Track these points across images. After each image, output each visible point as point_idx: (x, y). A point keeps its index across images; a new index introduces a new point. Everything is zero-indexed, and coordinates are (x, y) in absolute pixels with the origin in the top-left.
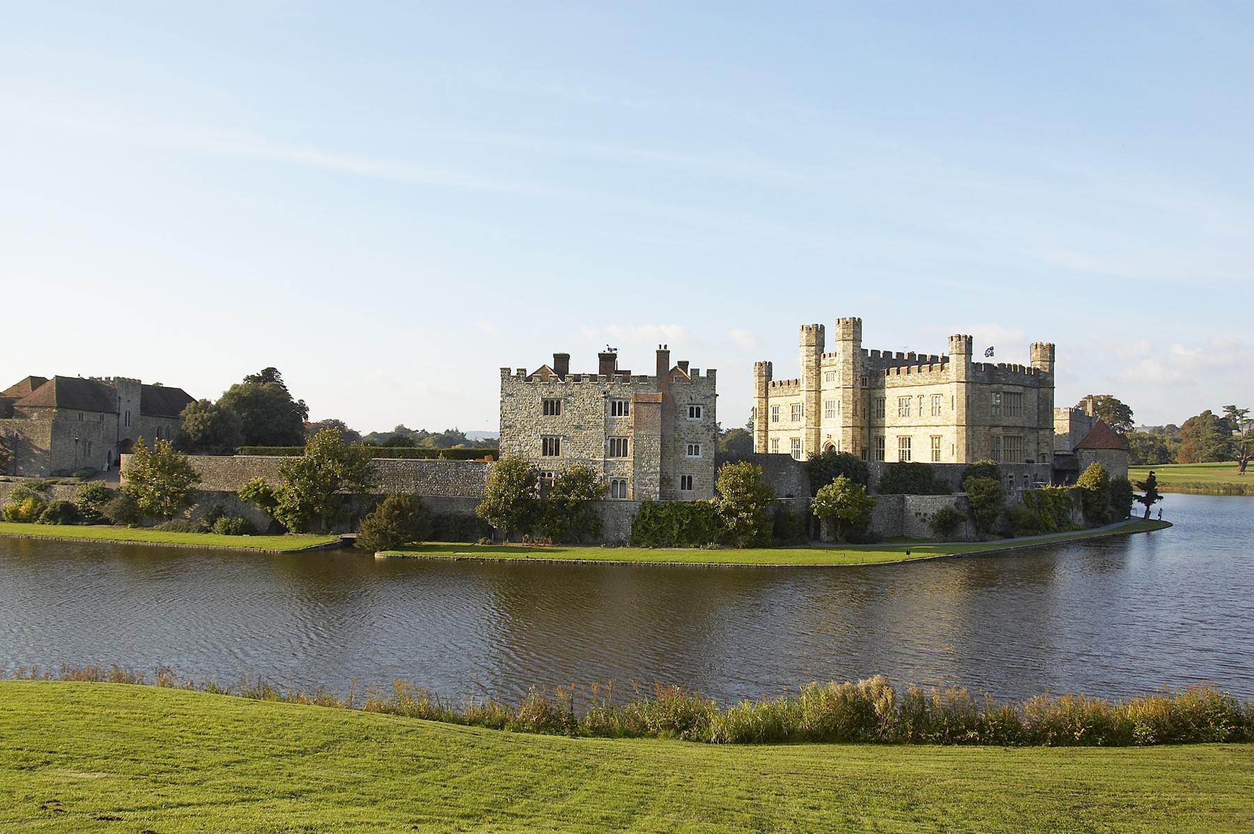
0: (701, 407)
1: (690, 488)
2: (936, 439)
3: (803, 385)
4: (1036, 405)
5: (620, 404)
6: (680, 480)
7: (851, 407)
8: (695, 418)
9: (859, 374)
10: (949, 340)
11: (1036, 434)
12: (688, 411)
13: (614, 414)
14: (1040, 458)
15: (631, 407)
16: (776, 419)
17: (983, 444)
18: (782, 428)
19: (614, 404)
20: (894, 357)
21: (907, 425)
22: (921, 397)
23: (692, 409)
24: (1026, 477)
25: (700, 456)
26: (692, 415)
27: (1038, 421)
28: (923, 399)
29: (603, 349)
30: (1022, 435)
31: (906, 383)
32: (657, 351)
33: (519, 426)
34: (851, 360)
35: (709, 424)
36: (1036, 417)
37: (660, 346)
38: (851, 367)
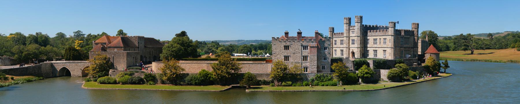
1: (324, 69)
3: (345, 35)
7: (360, 42)
9: (362, 32)
10: (389, 23)
11: (413, 49)
14: (414, 56)
15: (308, 47)
16: (335, 44)
18: (337, 47)
21: (376, 47)
22: (380, 39)
27: (414, 45)
28: (381, 40)
29: (298, 31)
30: (409, 49)
31: (376, 35)
32: (316, 33)
34: (359, 28)
36: (413, 44)
37: (316, 31)
38: (360, 30)
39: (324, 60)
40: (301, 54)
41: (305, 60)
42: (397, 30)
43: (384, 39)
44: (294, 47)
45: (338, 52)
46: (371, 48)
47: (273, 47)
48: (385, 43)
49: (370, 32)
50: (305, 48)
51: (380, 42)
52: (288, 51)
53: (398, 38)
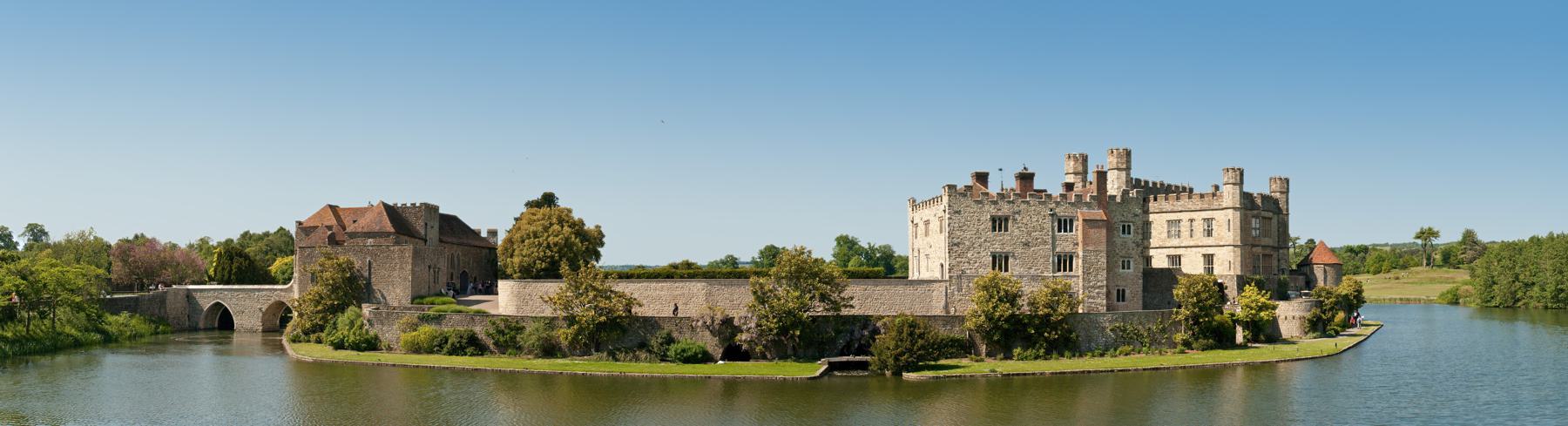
0: (1131, 224)
1: (1123, 300)
2: (1209, 259)
5: (1065, 221)
6: (1115, 292)
8: (1127, 235)
13: (1060, 231)
19: (1060, 221)
20: (1151, 185)
21: (1178, 245)
22: (1192, 220)
23: (1124, 227)
25: (1131, 270)
26: (1124, 232)
27: (1279, 242)
28: (1194, 223)
29: (1020, 170)
31: (1176, 209)
33: (967, 243)
39: (1123, 268)
41: (1065, 270)
42: (1244, 193)
43: (1205, 219)
44: (1025, 221)
46: (1159, 250)
48: (1209, 233)
49: (1155, 199)
51: (1192, 230)
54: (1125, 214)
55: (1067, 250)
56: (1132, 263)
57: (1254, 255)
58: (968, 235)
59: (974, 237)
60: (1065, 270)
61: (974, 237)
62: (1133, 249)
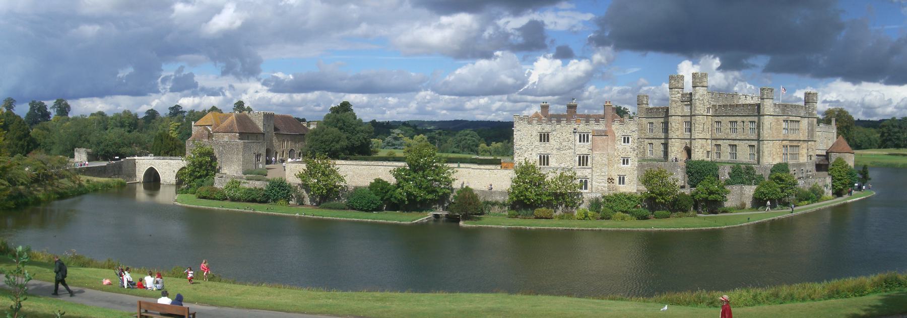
4: (807, 127)
5: (584, 135)
6: (618, 179)
7: (701, 127)
12: (623, 139)
14: (809, 157)
15: (590, 137)
17: (778, 150)
18: (655, 137)
23: (624, 138)
24: (802, 170)
26: (624, 142)
27: (808, 136)
33: (524, 148)
35: (634, 147)
36: (807, 134)
39: (624, 164)
40: (573, 151)
41: (583, 165)
44: (558, 136)
45: (657, 149)
46: (725, 141)
47: (517, 135)
50: (584, 138)
52: (547, 144)
53: (778, 121)
54: (625, 131)
55: (584, 153)
56: (629, 161)
57: (784, 146)
58: (525, 143)
59: (529, 145)
60: (583, 165)
61: (529, 145)
62: (631, 152)
